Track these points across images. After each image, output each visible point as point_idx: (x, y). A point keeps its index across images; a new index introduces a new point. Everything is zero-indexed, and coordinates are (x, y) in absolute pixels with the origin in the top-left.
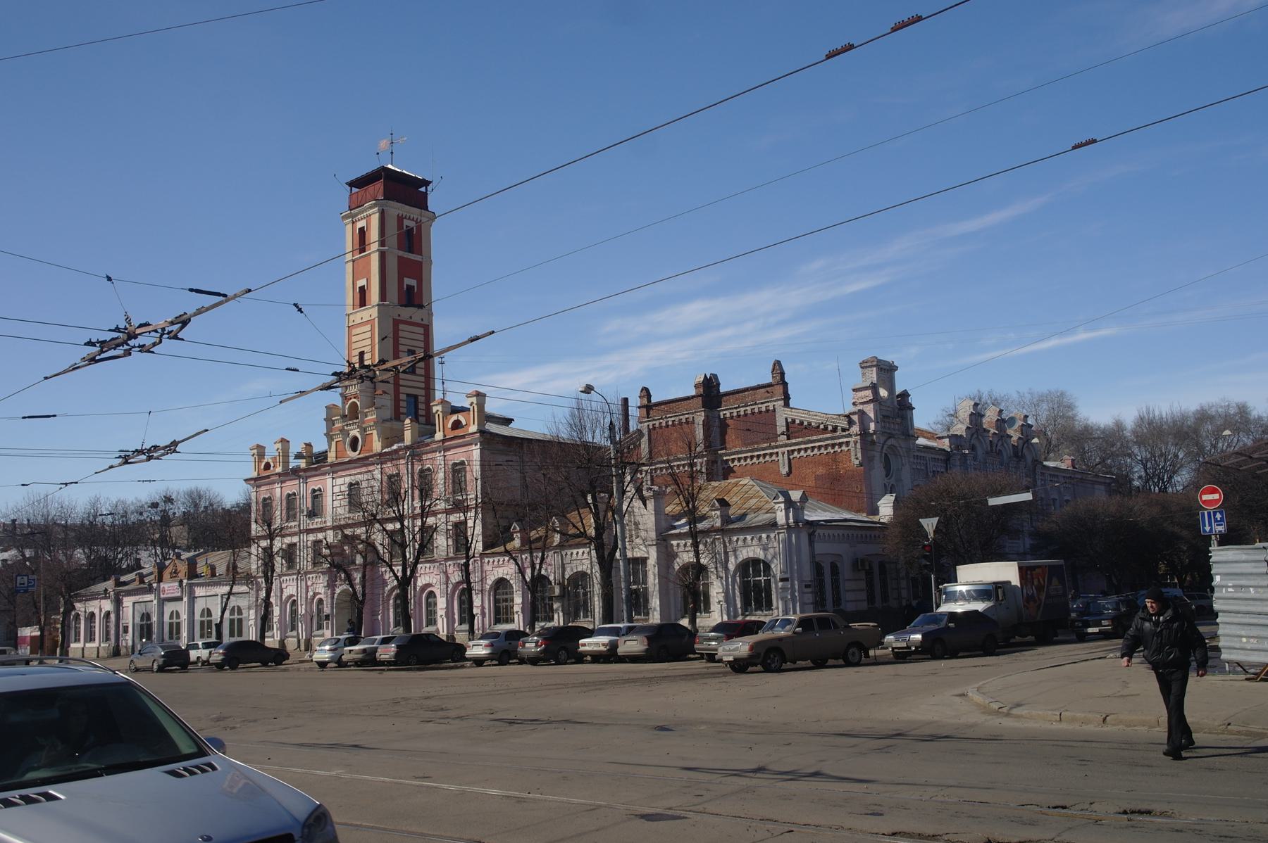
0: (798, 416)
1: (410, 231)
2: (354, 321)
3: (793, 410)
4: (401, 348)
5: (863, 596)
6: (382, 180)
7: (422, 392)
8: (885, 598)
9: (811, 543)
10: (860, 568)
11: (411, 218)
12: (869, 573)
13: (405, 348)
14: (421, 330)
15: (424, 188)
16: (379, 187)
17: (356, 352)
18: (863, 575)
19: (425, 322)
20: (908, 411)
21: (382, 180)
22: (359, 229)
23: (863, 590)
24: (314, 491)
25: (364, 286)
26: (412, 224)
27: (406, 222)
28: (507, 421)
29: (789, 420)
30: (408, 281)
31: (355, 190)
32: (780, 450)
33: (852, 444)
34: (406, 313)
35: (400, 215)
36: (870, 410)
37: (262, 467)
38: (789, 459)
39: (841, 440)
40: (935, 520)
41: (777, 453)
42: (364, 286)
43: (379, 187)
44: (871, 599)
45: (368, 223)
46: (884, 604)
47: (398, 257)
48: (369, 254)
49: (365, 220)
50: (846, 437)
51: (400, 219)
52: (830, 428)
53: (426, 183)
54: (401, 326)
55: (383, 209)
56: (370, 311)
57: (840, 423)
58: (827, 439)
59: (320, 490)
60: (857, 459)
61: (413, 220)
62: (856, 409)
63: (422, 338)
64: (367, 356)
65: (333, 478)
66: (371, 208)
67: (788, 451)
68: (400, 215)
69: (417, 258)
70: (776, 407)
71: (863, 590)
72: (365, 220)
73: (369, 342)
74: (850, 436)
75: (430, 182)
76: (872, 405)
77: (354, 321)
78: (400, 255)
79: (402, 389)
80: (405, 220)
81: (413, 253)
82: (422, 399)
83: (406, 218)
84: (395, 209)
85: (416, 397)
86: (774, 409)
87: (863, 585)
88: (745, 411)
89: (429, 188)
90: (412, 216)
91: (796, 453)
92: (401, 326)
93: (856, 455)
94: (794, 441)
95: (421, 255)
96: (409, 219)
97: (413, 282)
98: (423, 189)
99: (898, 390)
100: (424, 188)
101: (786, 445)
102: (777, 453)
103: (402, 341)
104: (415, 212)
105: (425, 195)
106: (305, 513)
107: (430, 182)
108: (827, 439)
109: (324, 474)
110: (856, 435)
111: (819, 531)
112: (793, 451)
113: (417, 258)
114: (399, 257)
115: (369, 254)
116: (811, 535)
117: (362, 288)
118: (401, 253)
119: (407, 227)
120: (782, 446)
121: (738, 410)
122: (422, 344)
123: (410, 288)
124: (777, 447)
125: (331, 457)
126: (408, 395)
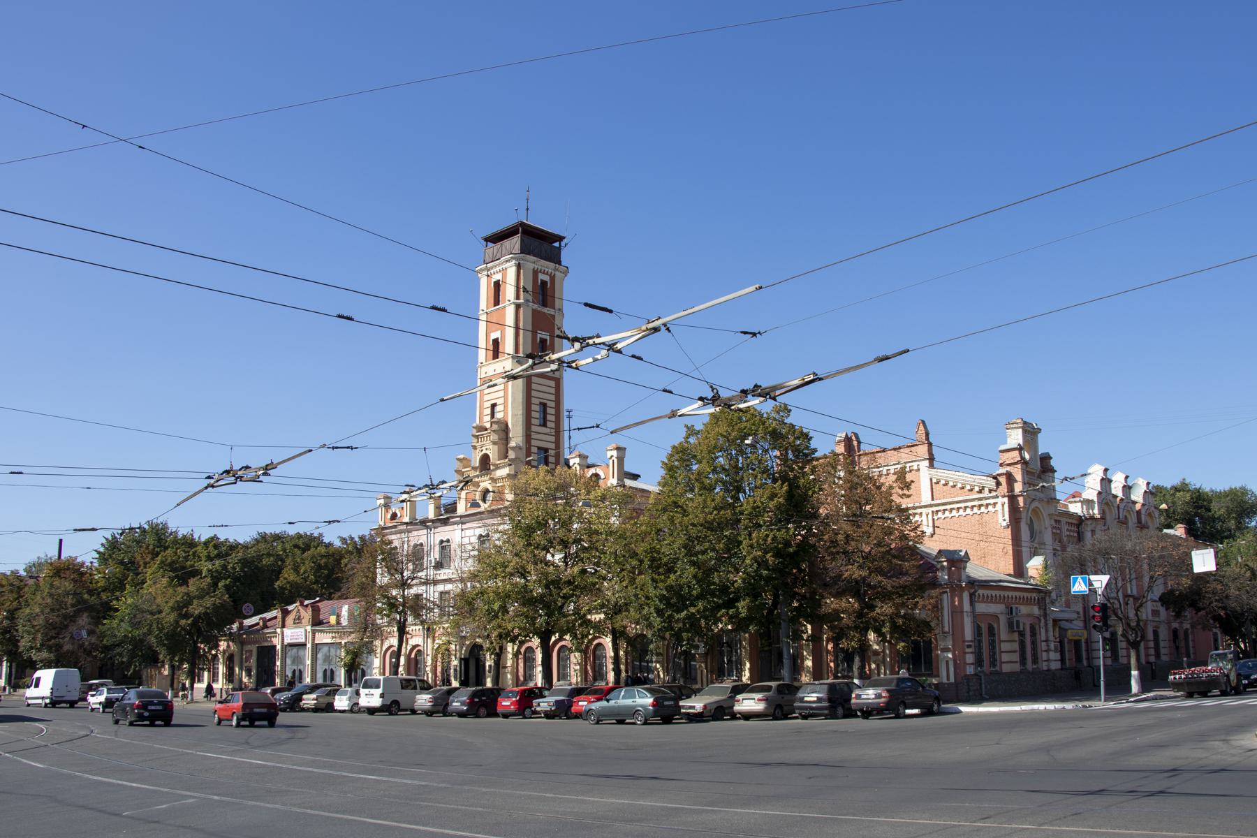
0: (943, 476)
1: (544, 283)
2: (486, 373)
3: (939, 470)
4: (533, 400)
5: (1016, 657)
6: (520, 235)
7: (552, 446)
8: (1035, 660)
9: (972, 603)
10: (1015, 629)
12: (1022, 634)
14: (552, 383)
15: (558, 243)
16: (515, 242)
17: (488, 404)
18: (1016, 636)
20: (1050, 474)
21: (520, 235)
22: (495, 282)
23: (1015, 652)
24: (442, 542)
25: (498, 338)
26: (546, 278)
27: (542, 277)
28: (635, 477)
29: (934, 480)
31: (490, 244)
32: (924, 511)
33: (999, 507)
36: (1017, 473)
37: (389, 516)
38: (933, 520)
39: (988, 501)
40: (1105, 579)
41: (921, 513)
42: (498, 338)
43: (515, 242)
44: (1023, 660)
45: (504, 276)
46: (1035, 666)
47: (533, 310)
48: (504, 307)
49: (501, 274)
50: (993, 498)
51: (535, 273)
52: (977, 489)
53: (560, 239)
54: (534, 379)
55: (519, 263)
56: (503, 364)
57: (988, 484)
58: (973, 500)
59: (448, 541)
60: (1004, 520)
61: (547, 274)
62: (1003, 470)
63: (553, 391)
64: (498, 409)
65: (462, 530)
66: (508, 261)
67: (933, 512)
69: (551, 312)
70: (920, 467)
71: (1015, 652)
72: (501, 274)
73: (502, 394)
74: (997, 497)
75: (564, 238)
76: (1019, 466)
77: (486, 373)
78: (534, 308)
79: (533, 442)
80: (540, 274)
81: (546, 307)
82: (552, 452)
83: (540, 272)
84: (532, 262)
85: (546, 450)
86: (918, 470)
87: (1016, 646)
88: (887, 470)
89: (563, 244)
90: (547, 270)
91: (940, 513)
93: (1004, 516)
94: (939, 502)
95: (554, 309)
96: (544, 273)
98: (557, 244)
99: (1041, 450)
100: (558, 243)
101: (931, 506)
102: (921, 513)
103: (534, 393)
104: (549, 266)
105: (559, 249)
106: (433, 564)
107: (564, 238)
108: (973, 500)
109: (454, 523)
110: (1004, 496)
111: (981, 592)
112: (937, 511)
113: (551, 312)
114: (534, 311)
115: (504, 307)
116: (971, 595)
117: (496, 342)
118: (535, 306)
119: (541, 280)
120: (926, 506)
121: (881, 469)
122: (553, 397)
123: (543, 341)
124: (920, 507)
125: (461, 509)
126: (539, 448)
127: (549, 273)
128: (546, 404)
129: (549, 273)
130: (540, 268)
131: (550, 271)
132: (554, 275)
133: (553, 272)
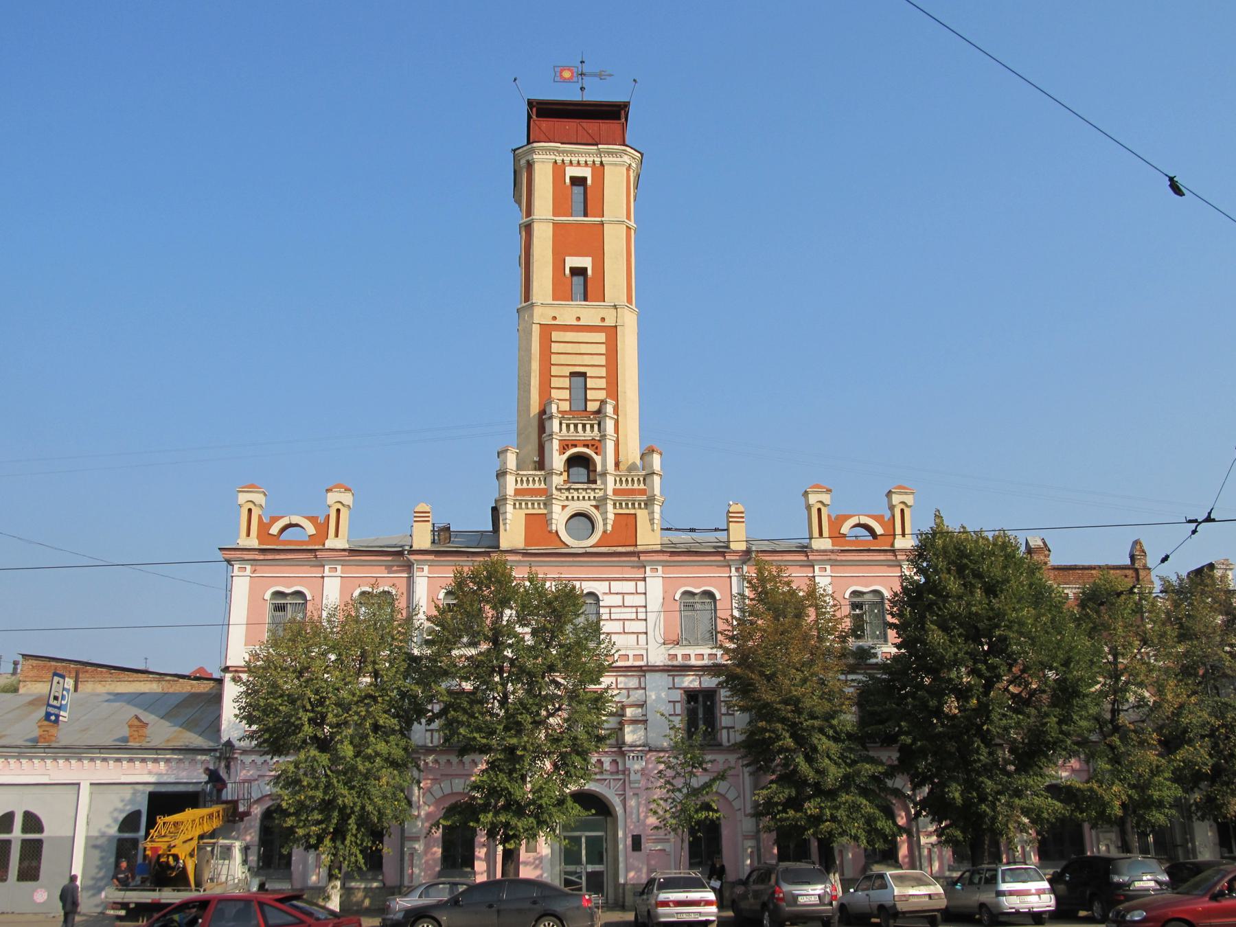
1: (578, 181)
4: (554, 371)
11: (582, 162)
13: (566, 371)
14: (601, 337)
19: (610, 322)
27: (571, 172)
30: (572, 262)
34: (570, 312)
35: (559, 162)
51: (558, 169)
54: (555, 336)
63: (602, 349)
68: (559, 162)
80: (568, 169)
90: (582, 160)
92: (555, 336)
97: (585, 262)
103: (554, 359)
123: (579, 272)
127: (590, 163)
128: (585, 373)
129: (590, 163)
130: (567, 159)
131: (590, 160)
132: (601, 162)
133: (598, 160)
